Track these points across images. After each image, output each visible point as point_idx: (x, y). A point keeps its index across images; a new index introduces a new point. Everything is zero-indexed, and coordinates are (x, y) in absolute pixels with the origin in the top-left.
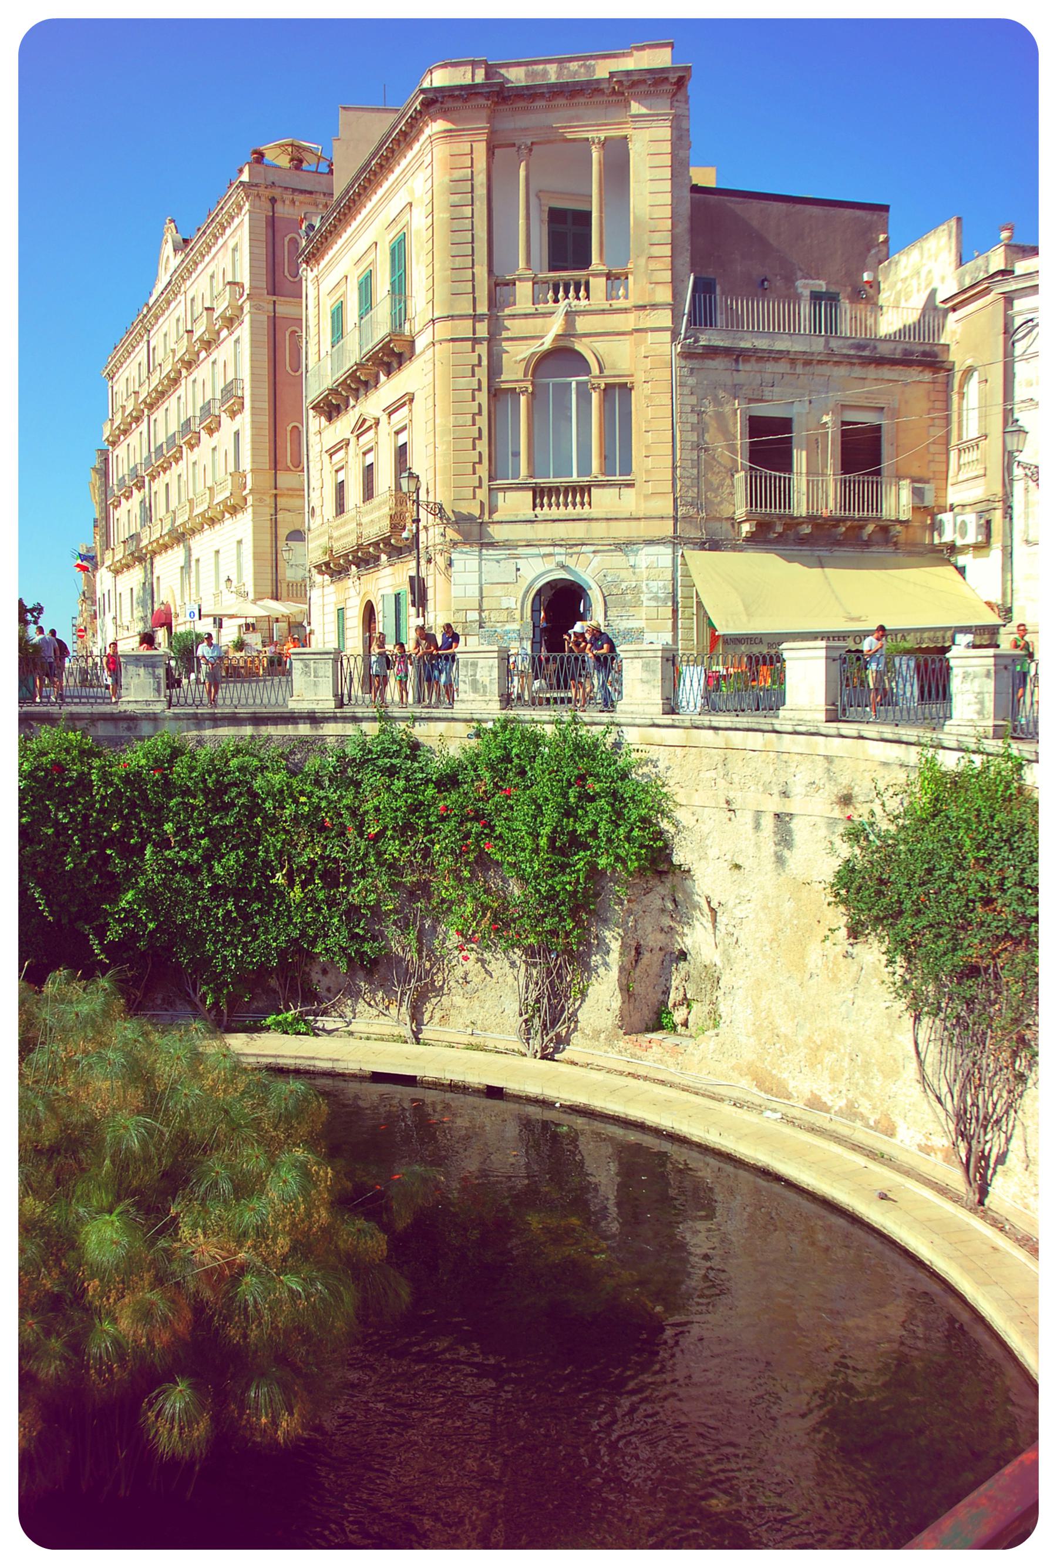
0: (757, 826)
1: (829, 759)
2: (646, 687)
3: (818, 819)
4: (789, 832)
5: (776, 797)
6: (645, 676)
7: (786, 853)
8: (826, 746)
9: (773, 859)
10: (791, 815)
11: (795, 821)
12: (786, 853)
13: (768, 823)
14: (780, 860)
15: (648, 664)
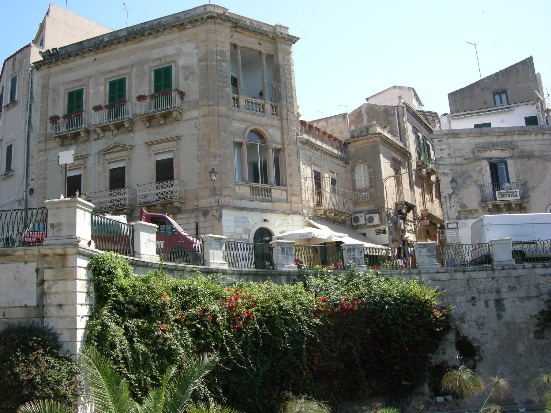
0: (487, 305)
1: (516, 277)
2: (430, 258)
3: (514, 299)
4: (503, 305)
5: (495, 294)
6: (429, 254)
7: (502, 313)
8: (516, 273)
9: (496, 316)
10: (503, 299)
11: (505, 301)
12: (502, 313)
13: (492, 304)
14: (499, 317)
15: (430, 249)
